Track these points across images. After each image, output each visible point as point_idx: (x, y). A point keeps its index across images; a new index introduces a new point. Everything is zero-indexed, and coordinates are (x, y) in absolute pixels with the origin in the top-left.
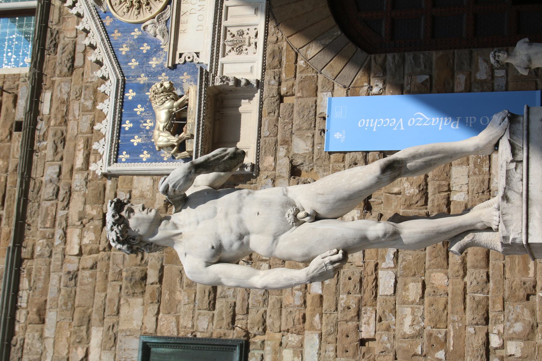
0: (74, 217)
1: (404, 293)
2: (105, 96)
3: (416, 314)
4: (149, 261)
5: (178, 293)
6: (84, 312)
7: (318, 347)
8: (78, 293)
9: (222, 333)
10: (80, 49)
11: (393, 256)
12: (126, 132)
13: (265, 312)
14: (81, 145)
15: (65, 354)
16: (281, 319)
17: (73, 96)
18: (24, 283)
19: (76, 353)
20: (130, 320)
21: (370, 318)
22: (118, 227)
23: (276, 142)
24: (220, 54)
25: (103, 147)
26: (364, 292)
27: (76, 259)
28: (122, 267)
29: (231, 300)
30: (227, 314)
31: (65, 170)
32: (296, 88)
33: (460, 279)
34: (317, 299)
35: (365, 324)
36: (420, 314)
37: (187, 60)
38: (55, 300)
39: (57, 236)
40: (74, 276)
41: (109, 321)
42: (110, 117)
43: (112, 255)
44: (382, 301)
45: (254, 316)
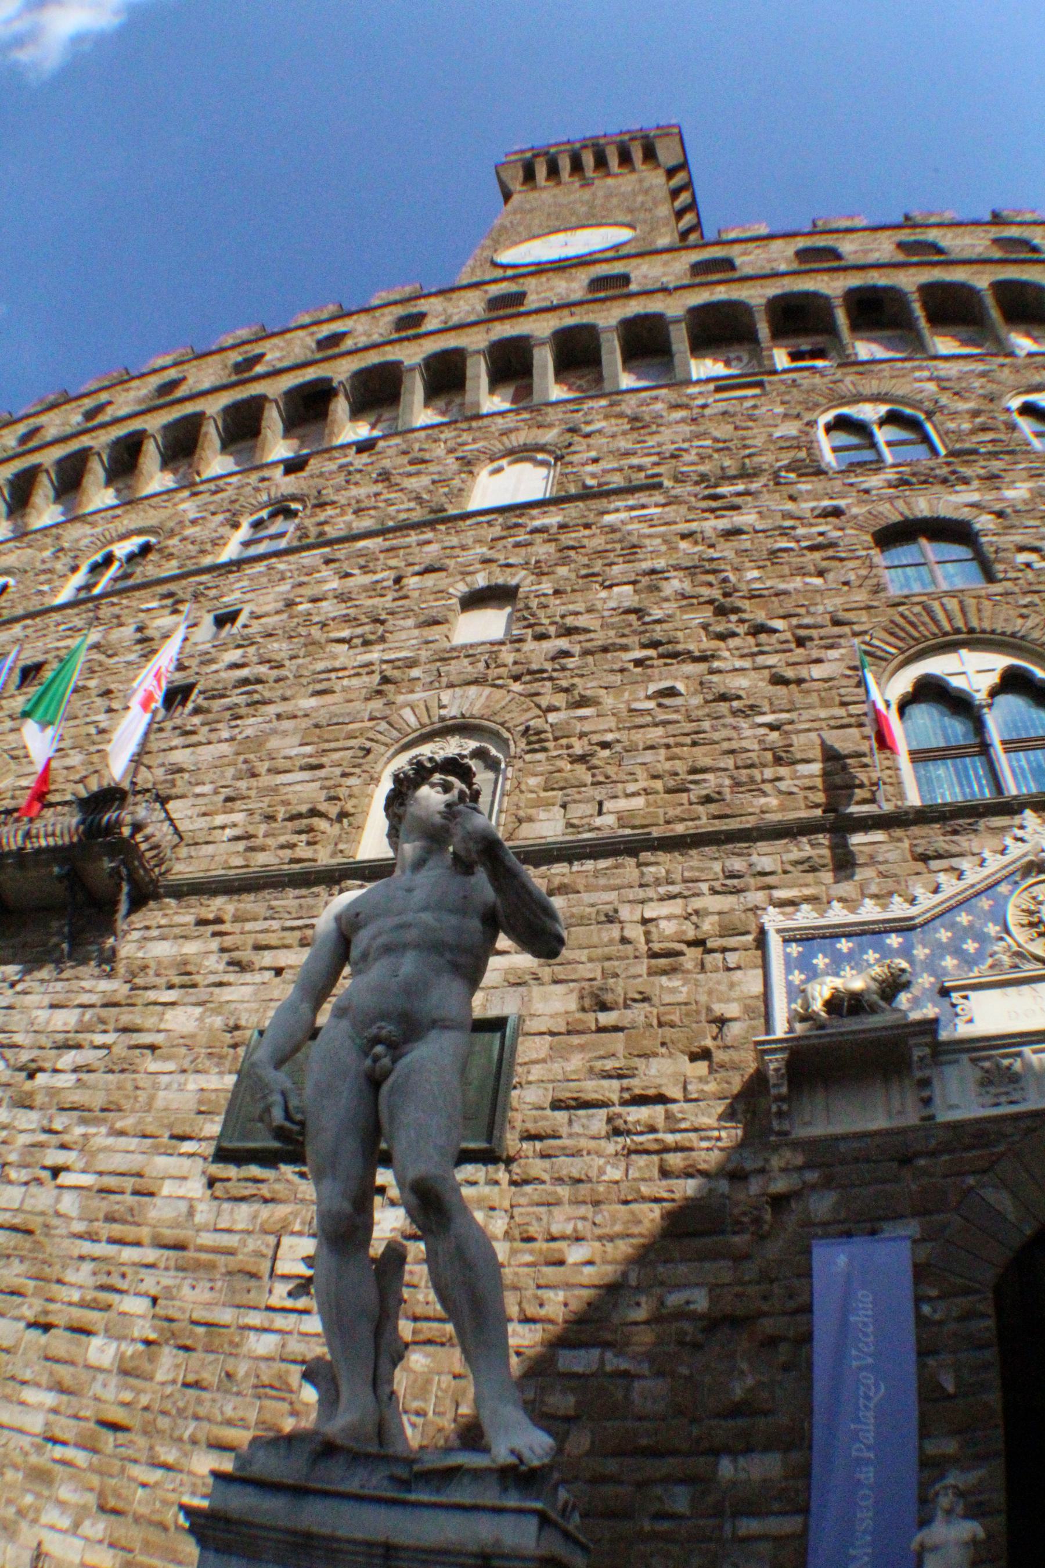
0: (697, 903)
2: (885, 907)
10: (954, 862)
12: (833, 945)
13: (543, 1182)
14: (807, 892)
17: (881, 868)
18: (603, 864)
20: (545, 998)
21: (523, 1337)
23: (829, 1165)
24: (975, 1055)
25: (806, 917)
27: (637, 917)
29: (564, 1131)
31: (769, 880)
32: (925, 1181)
34: (557, 1256)
37: (958, 1009)
38: (579, 903)
39: (670, 888)
40: (611, 918)
42: (852, 918)
45: (538, 1168)
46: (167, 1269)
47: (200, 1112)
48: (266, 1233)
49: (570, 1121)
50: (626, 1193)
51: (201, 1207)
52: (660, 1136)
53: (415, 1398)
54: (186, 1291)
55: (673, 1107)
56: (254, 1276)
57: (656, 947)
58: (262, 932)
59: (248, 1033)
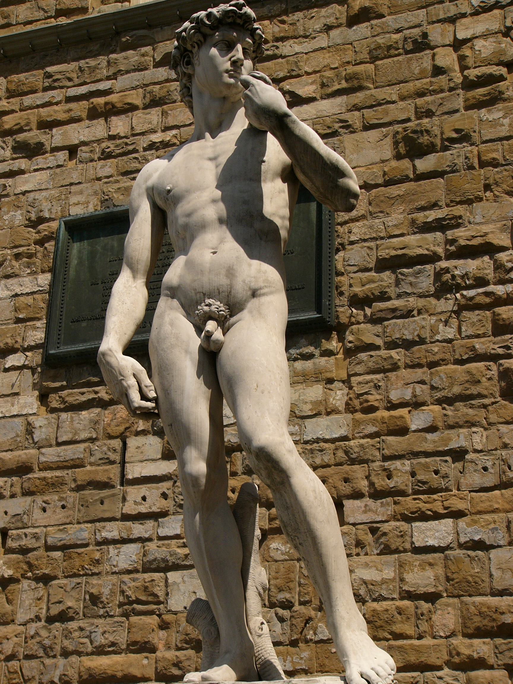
1: (417, 563)
3: (384, 586)
4: (450, 152)
5: (402, 208)
6: (368, 77)
7: (327, 437)
8: (395, 59)
9: (342, 289)
11: (476, 538)
13: (378, 348)
15: (307, 69)
16: (368, 373)
19: (308, 84)
21: (375, 512)
22: (192, 28)
26: (415, 499)
27: (449, 39)
28: (438, 113)
29: (392, 291)
30: (370, 290)
33: (446, 657)
35: (366, 506)
36: (384, 593)
40: (422, 44)
41: (355, 118)
43: (458, 91)
44: (402, 529)
46: (13, 496)
47: (18, 321)
48: (111, 437)
49: (398, 283)
50: (461, 353)
51: (38, 422)
52: (491, 288)
53: (280, 590)
54: (37, 514)
55: (503, 256)
56: (106, 485)
57: (473, 73)
58: (43, 106)
59: (54, 225)
